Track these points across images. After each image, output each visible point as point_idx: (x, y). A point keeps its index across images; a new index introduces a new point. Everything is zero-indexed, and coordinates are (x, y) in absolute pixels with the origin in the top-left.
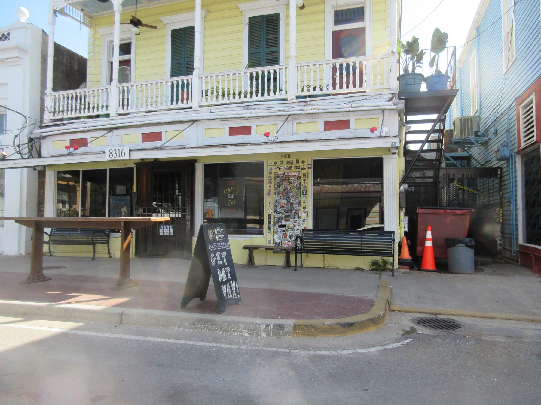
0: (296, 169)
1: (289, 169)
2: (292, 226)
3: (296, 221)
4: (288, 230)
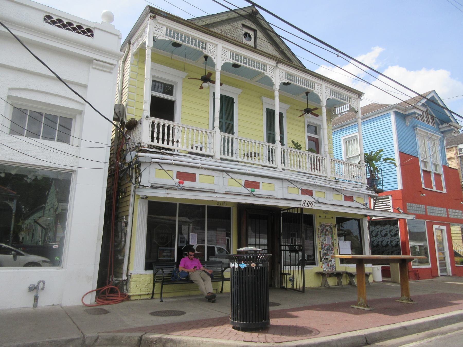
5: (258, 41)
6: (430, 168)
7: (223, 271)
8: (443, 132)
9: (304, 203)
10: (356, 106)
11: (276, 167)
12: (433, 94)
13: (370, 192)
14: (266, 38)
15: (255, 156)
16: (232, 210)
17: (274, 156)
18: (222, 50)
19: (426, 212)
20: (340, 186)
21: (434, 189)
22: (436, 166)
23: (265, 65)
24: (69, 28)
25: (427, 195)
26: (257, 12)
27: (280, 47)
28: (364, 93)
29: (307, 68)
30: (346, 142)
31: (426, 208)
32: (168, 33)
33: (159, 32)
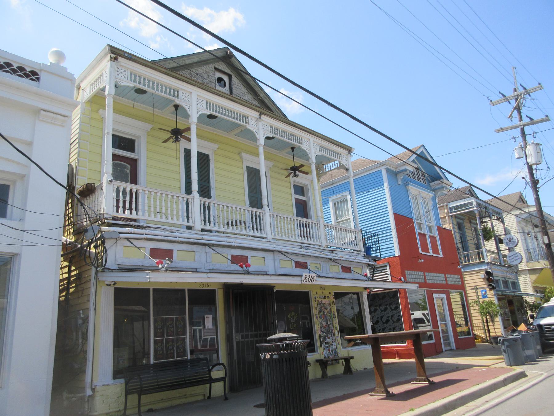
2: (331, 342)
4: (330, 346)
5: (233, 87)
6: (425, 231)
7: (210, 371)
8: (434, 190)
9: (306, 278)
10: (347, 163)
11: (266, 236)
12: (422, 149)
13: (369, 260)
14: (242, 84)
15: (236, 225)
16: (218, 293)
17: (262, 224)
18: (198, 99)
19: (425, 279)
20: (336, 255)
21: (431, 253)
22: (430, 228)
23: (247, 117)
24: (8, 69)
25: (424, 260)
26: (231, 56)
27: (259, 95)
28: (355, 149)
29: (290, 119)
30: (335, 204)
31: (424, 275)
32: (133, 78)
33: (121, 76)
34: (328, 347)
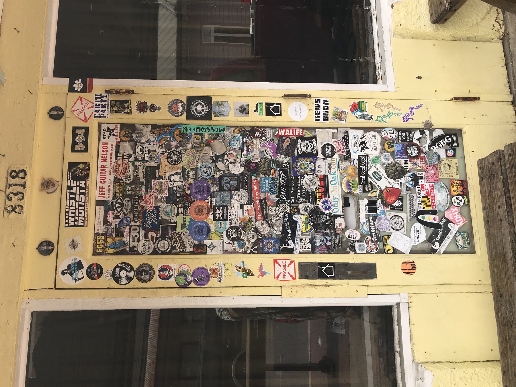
0: (86, 143)
1: (85, 178)
2: (346, 164)
3: (324, 148)
34: (372, 207)
